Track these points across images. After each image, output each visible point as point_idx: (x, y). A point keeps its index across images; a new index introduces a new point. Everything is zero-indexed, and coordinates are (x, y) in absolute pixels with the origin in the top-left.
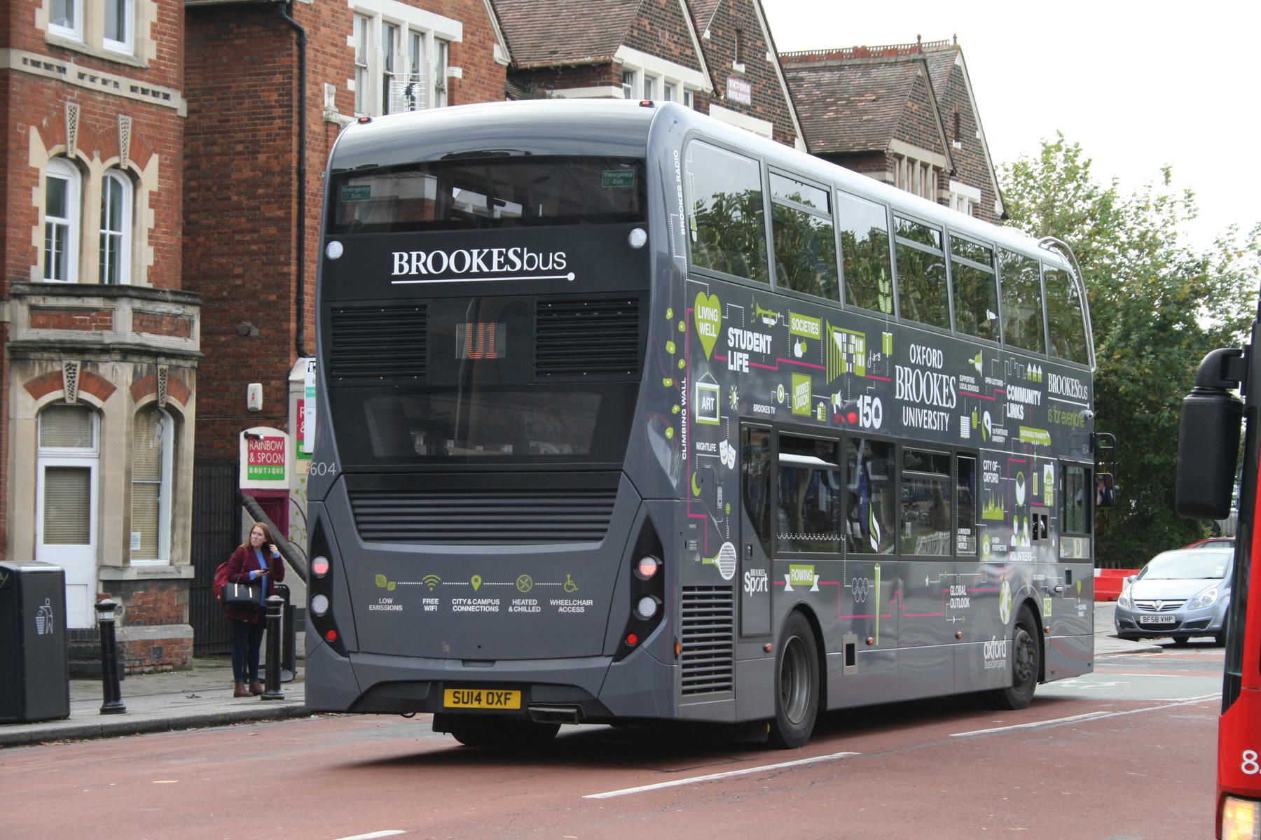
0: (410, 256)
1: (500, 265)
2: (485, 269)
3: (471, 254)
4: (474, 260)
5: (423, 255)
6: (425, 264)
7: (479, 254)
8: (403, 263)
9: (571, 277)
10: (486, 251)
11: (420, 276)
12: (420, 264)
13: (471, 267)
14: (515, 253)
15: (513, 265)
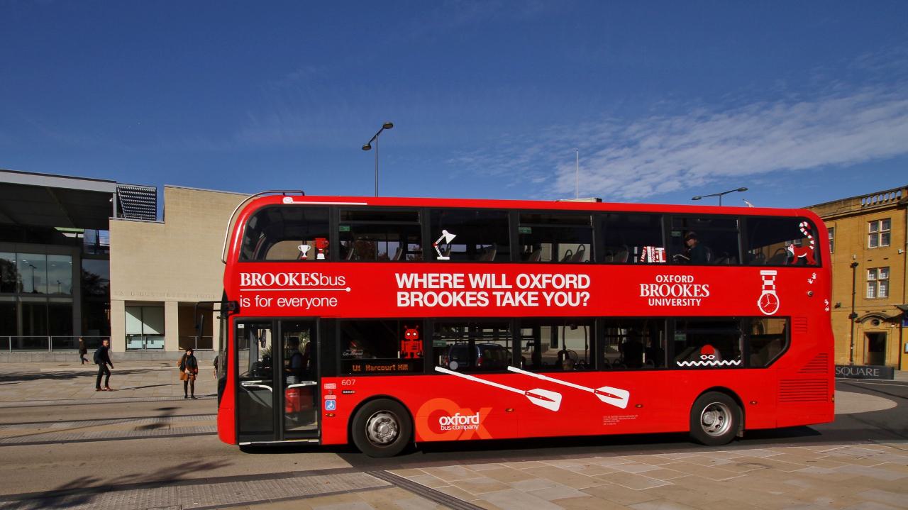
0: (251, 276)
1: (307, 282)
2: (298, 284)
3: (289, 276)
5: (259, 275)
6: (260, 280)
7: (294, 276)
8: (247, 279)
9: (348, 290)
10: (297, 274)
12: (258, 280)
13: (289, 283)
14: (315, 276)
15: (314, 282)
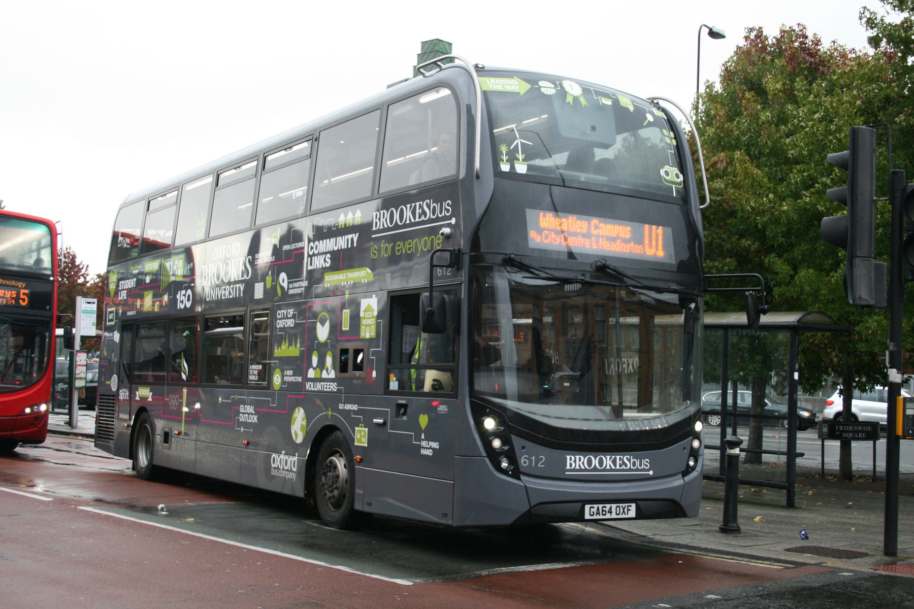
1: (620, 466)
4: (608, 461)
9: (651, 473)
11: (580, 470)
15: (626, 466)
